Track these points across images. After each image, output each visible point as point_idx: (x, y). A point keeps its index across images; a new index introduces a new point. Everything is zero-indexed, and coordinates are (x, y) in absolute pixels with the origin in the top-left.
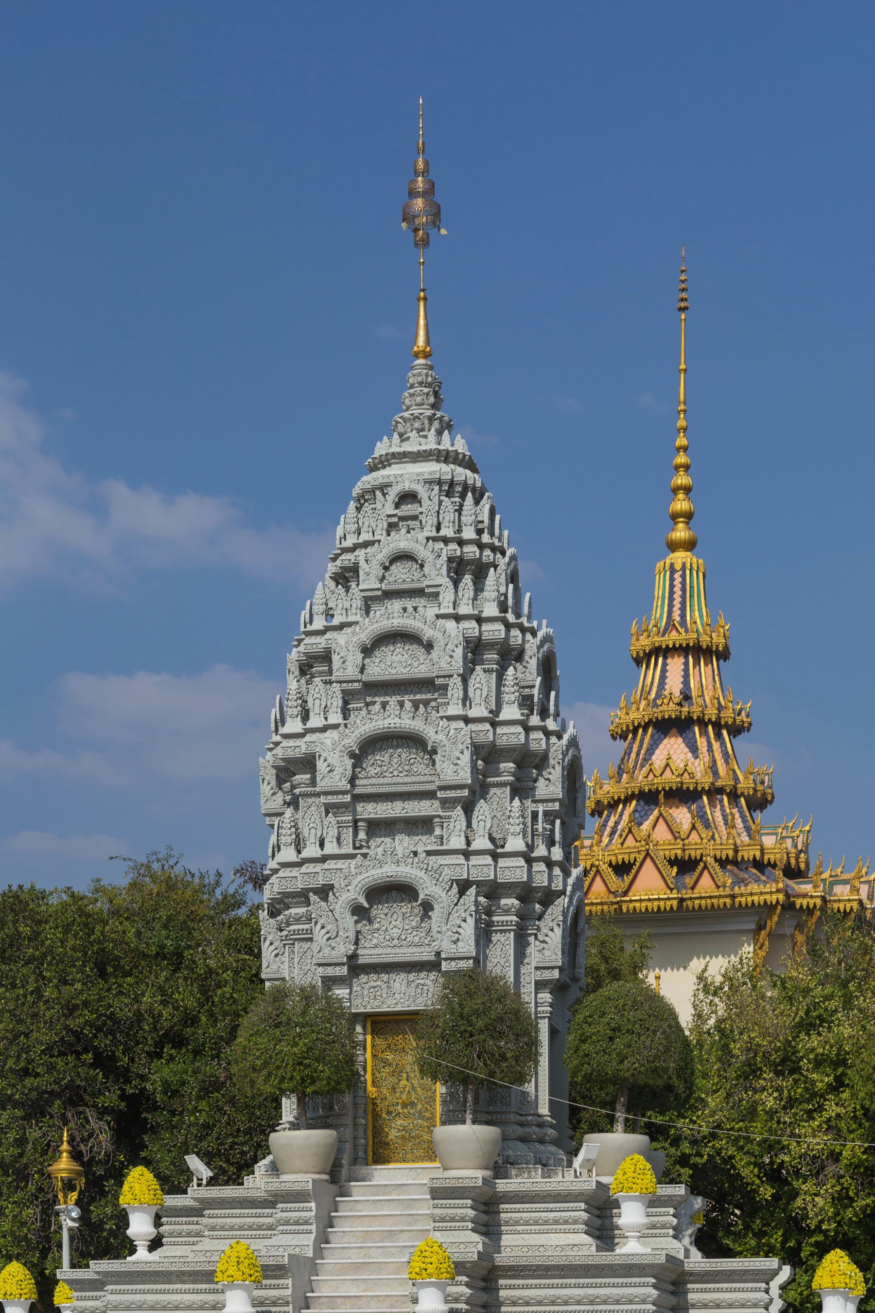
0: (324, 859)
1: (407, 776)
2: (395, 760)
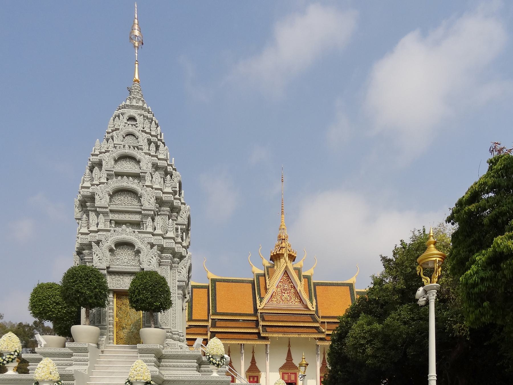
0: (99, 231)
1: (130, 205)
2: (126, 199)
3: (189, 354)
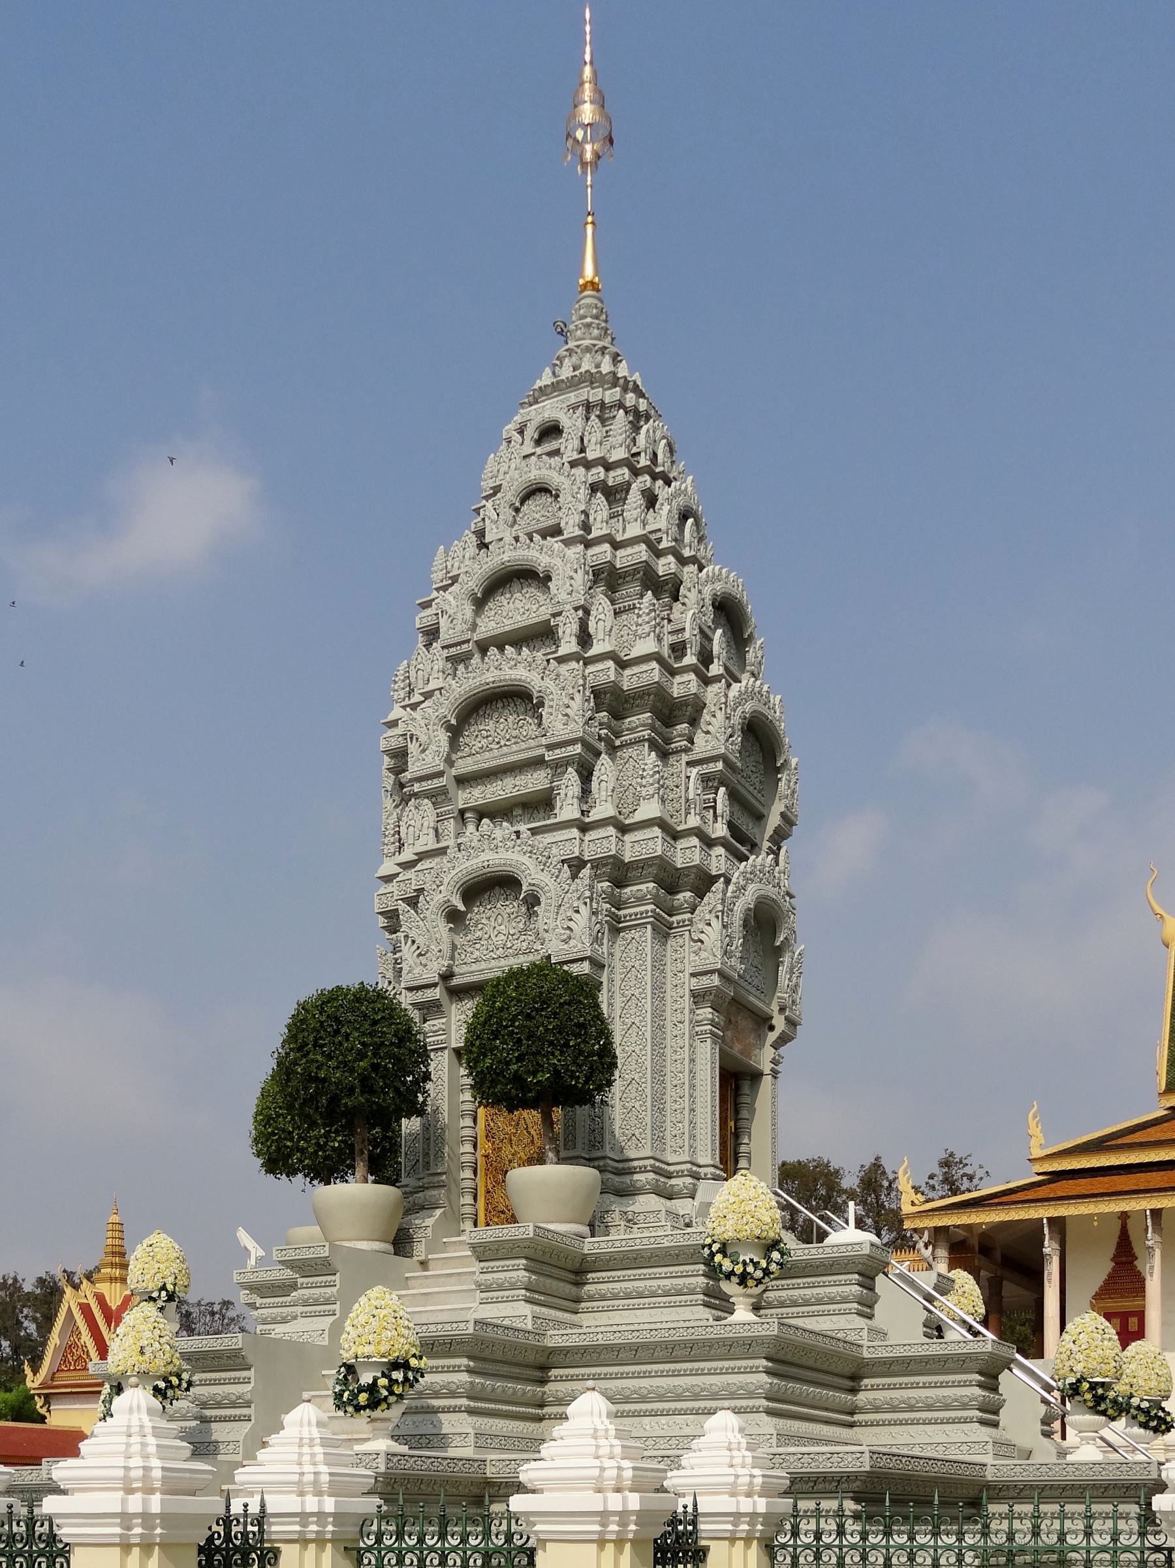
1: (516, 743)
3: (672, 1244)
